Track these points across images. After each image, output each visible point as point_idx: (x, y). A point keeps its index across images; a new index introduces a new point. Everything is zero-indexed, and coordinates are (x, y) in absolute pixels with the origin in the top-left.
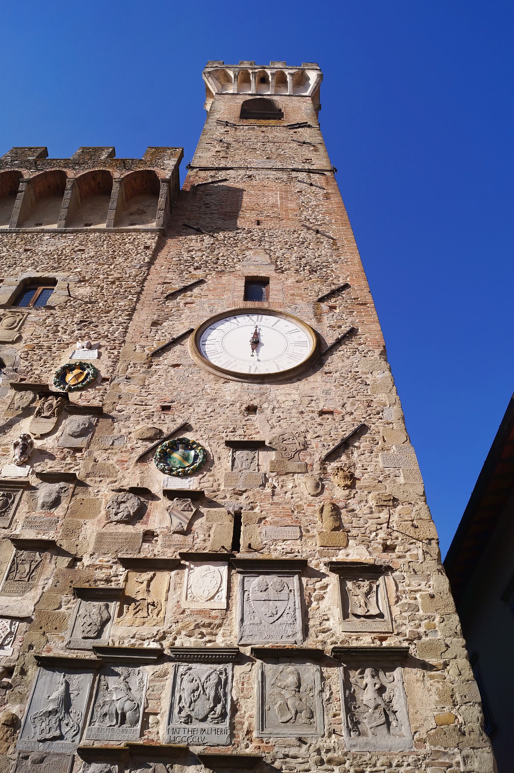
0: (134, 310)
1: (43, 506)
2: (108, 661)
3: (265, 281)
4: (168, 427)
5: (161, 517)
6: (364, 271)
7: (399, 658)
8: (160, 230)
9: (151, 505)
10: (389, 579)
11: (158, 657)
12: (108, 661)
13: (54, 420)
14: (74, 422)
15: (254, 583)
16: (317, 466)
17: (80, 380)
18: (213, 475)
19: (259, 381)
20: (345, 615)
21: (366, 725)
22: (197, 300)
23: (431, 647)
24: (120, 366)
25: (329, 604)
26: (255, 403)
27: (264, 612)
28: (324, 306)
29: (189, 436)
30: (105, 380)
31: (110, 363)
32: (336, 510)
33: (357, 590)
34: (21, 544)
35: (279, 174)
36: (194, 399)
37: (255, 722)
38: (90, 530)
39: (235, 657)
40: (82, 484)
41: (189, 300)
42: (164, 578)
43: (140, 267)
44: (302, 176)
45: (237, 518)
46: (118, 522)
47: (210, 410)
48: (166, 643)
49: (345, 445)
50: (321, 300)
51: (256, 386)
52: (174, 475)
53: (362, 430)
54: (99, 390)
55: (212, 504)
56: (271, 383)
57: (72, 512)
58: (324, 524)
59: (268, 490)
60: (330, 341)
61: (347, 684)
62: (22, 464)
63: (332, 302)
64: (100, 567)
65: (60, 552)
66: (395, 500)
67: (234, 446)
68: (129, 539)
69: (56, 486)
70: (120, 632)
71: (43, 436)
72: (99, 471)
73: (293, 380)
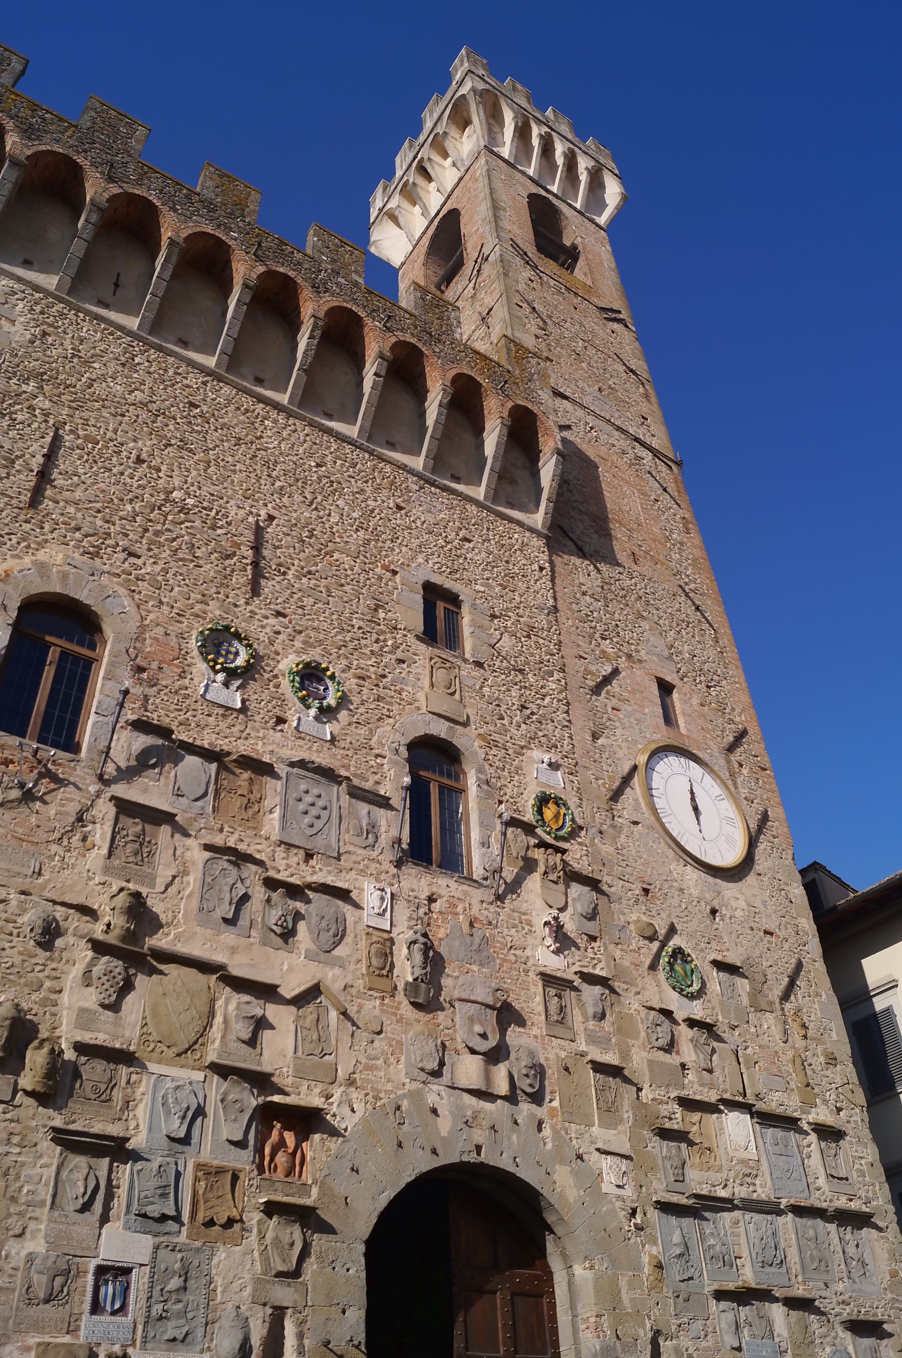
1: (595, 1017)
6: (754, 707)
17: (561, 823)
18: (709, 1001)
19: (713, 873)
26: (716, 904)
35: (623, 443)
36: (666, 885)
37: (798, 1266)
41: (615, 702)
43: (548, 614)
44: (648, 456)
46: (659, 1048)
47: (684, 906)
51: (710, 879)
52: (683, 995)
54: (580, 844)
56: (723, 878)
57: (620, 1030)
60: (753, 826)
62: (557, 952)
73: (737, 878)
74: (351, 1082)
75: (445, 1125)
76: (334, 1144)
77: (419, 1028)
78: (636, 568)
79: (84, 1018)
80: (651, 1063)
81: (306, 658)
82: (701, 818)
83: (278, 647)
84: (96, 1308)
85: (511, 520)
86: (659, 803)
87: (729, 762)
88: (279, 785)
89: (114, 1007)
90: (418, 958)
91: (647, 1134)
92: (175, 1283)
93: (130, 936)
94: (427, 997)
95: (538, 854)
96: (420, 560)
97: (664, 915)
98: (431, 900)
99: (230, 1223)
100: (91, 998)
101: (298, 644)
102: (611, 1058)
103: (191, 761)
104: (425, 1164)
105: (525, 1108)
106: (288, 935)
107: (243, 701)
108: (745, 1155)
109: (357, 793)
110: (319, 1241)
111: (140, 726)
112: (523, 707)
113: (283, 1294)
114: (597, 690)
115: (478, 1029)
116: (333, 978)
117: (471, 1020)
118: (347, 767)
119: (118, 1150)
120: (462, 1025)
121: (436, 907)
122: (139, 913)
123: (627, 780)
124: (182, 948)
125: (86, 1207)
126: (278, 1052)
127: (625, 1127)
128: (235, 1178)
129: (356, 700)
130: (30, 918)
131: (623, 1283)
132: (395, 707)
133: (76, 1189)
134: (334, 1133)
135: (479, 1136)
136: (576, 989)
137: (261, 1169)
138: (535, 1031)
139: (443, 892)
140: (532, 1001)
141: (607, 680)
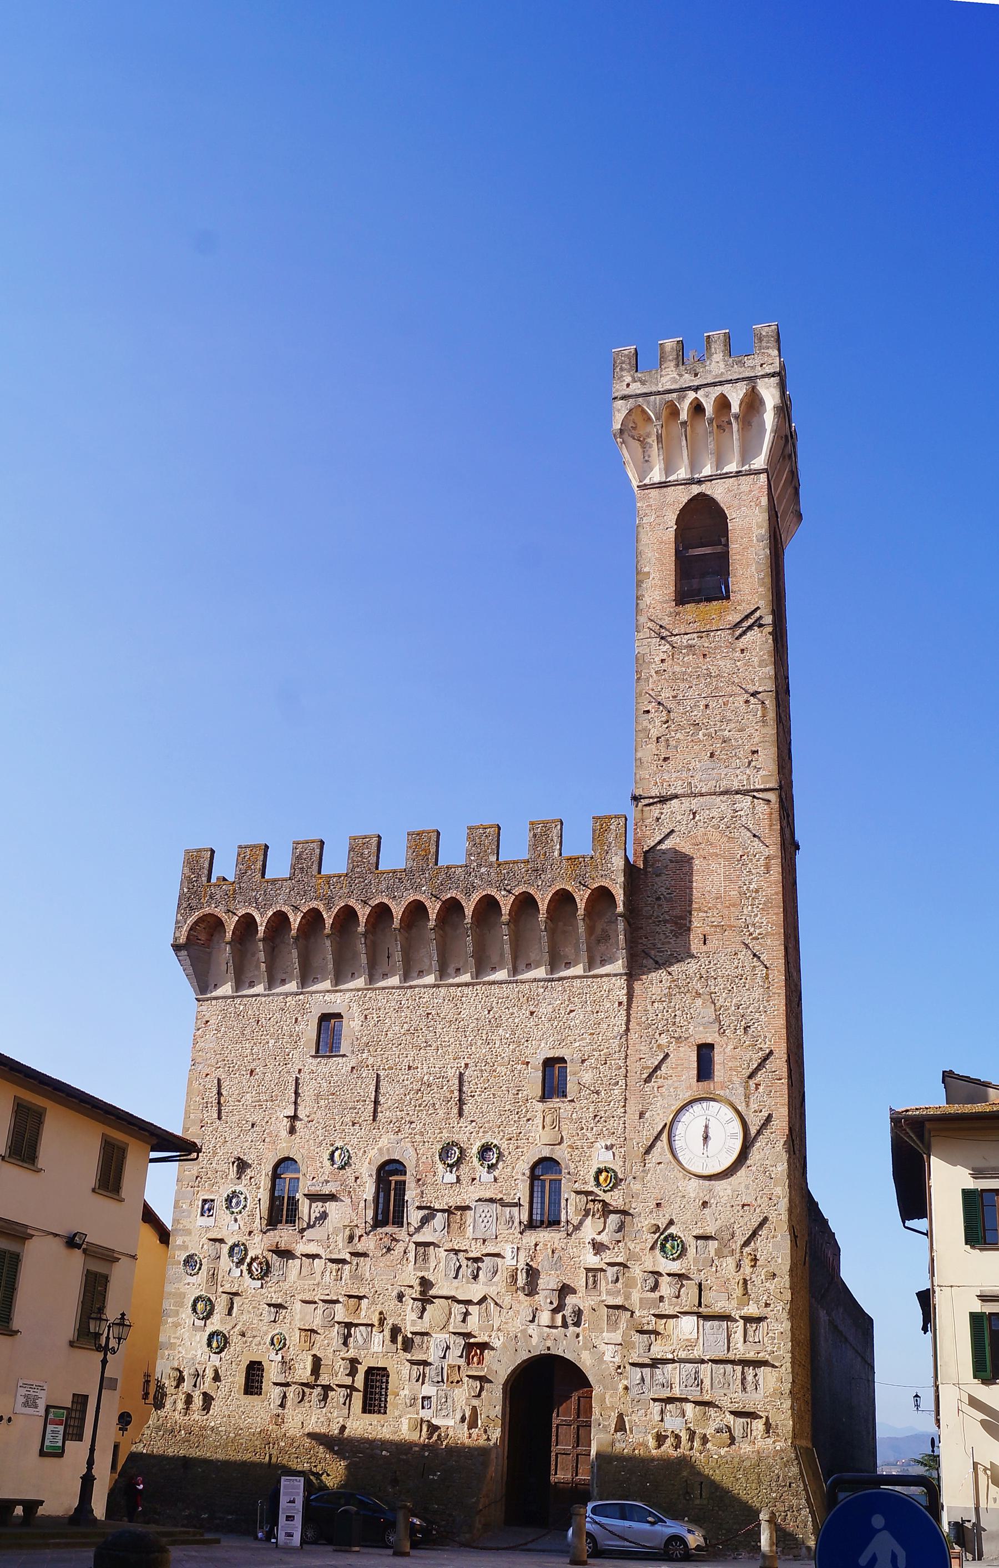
0: (626, 1099)
2: (655, 1363)
3: (711, 1047)
4: (662, 1223)
5: (666, 1287)
7: (765, 1363)
8: (626, 974)
9: (660, 1279)
10: (765, 1324)
11: (673, 1361)
12: (655, 1363)
13: (602, 1219)
14: (613, 1219)
15: (709, 1324)
16: (738, 1251)
20: (745, 1342)
21: (748, 1389)
22: (666, 1082)
23: (777, 1358)
24: (628, 1165)
25: (738, 1336)
26: (706, 1199)
27: (711, 1340)
28: (752, 1083)
29: (672, 1230)
30: (621, 1180)
31: (622, 1163)
32: (745, 1281)
33: (751, 1328)
34: (608, 1307)
38: (636, 1296)
39: (703, 1362)
40: (625, 1266)
42: (671, 1322)
45: (700, 1285)
48: (675, 1354)
49: (754, 1234)
50: (751, 1076)
51: (707, 1183)
53: (766, 1219)
55: (688, 1278)
57: (626, 1285)
58: (739, 1292)
59: (714, 1269)
60: (753, 1131)
61: (743, 1373)
62: (595, 1254)
63: (759, 1077)
64: (645, 1317)
65: (626, 1309)
66: (775, 1275)
67: (697, 1238)
68: (653, 1300)
69: (616, 1268)
70: (658, 1350)
71: (599, 1233)
72: (632, 1256)
74: (499, 1330)
75: (534, 1341)
76: (492, 1353)
77: (526, 1304)
78: (705, 948)
79: (413, 1323)
80: (641, 1299)
81: (483, 1141)
82: (710, 1143)
83: (472, 1141)
84: (423, 1408)
85: (602, 976)
86: (678, 1144)
87: (747, 1088)
88: (472, 1212)
89: (421, 1317)
90: (524, 1275)
91: (633, 1333)
92: (444, 1400)
93: (423, 1293)
94: (531, 1289)
95: (590, 1205)
96: (543, 1045)
97: (667, 1216)
98: (536, 1245)
99: (458, 1382)
100: (414, 1316)
101: (481, 1134)
102: (618, 1301)
103: (439, 1214)
104: (525, 1356)
105: (571, 1329)
106: (475, 1277)
107: (458, 1177)
108: (690, 1337)
109: (505, 1205)
110: (486, 1386)
111: (419, 1208)
112: (596, 1116)
113: (475, 1402)
114: (647, 1080)
115: (549, 1301)
116: (492, 1291)
117: (546, 1297)
118: (501, 1192)
119: (425, 1363)
120: (544, 1299)
121: (538, 1248)
122: (425, 1284)
123: (657, 1138)
124: (441, 1293)
125: (417, 1381)
126: (473, 1324)
127: (620, 1332)
128: (459, 1367)
129: (506, 1153)
130: (395, 1293)
131: (607, 1396)
132: (525, 1150)
133: (414, 1375)
134: (493, 1349)
135: (549, 1343)
136: (605, 1271)
137: (468, 1364)
138: (580, 1295)
139: (542, 1240)
140: (579, 1282)
141: (658, 1068)
